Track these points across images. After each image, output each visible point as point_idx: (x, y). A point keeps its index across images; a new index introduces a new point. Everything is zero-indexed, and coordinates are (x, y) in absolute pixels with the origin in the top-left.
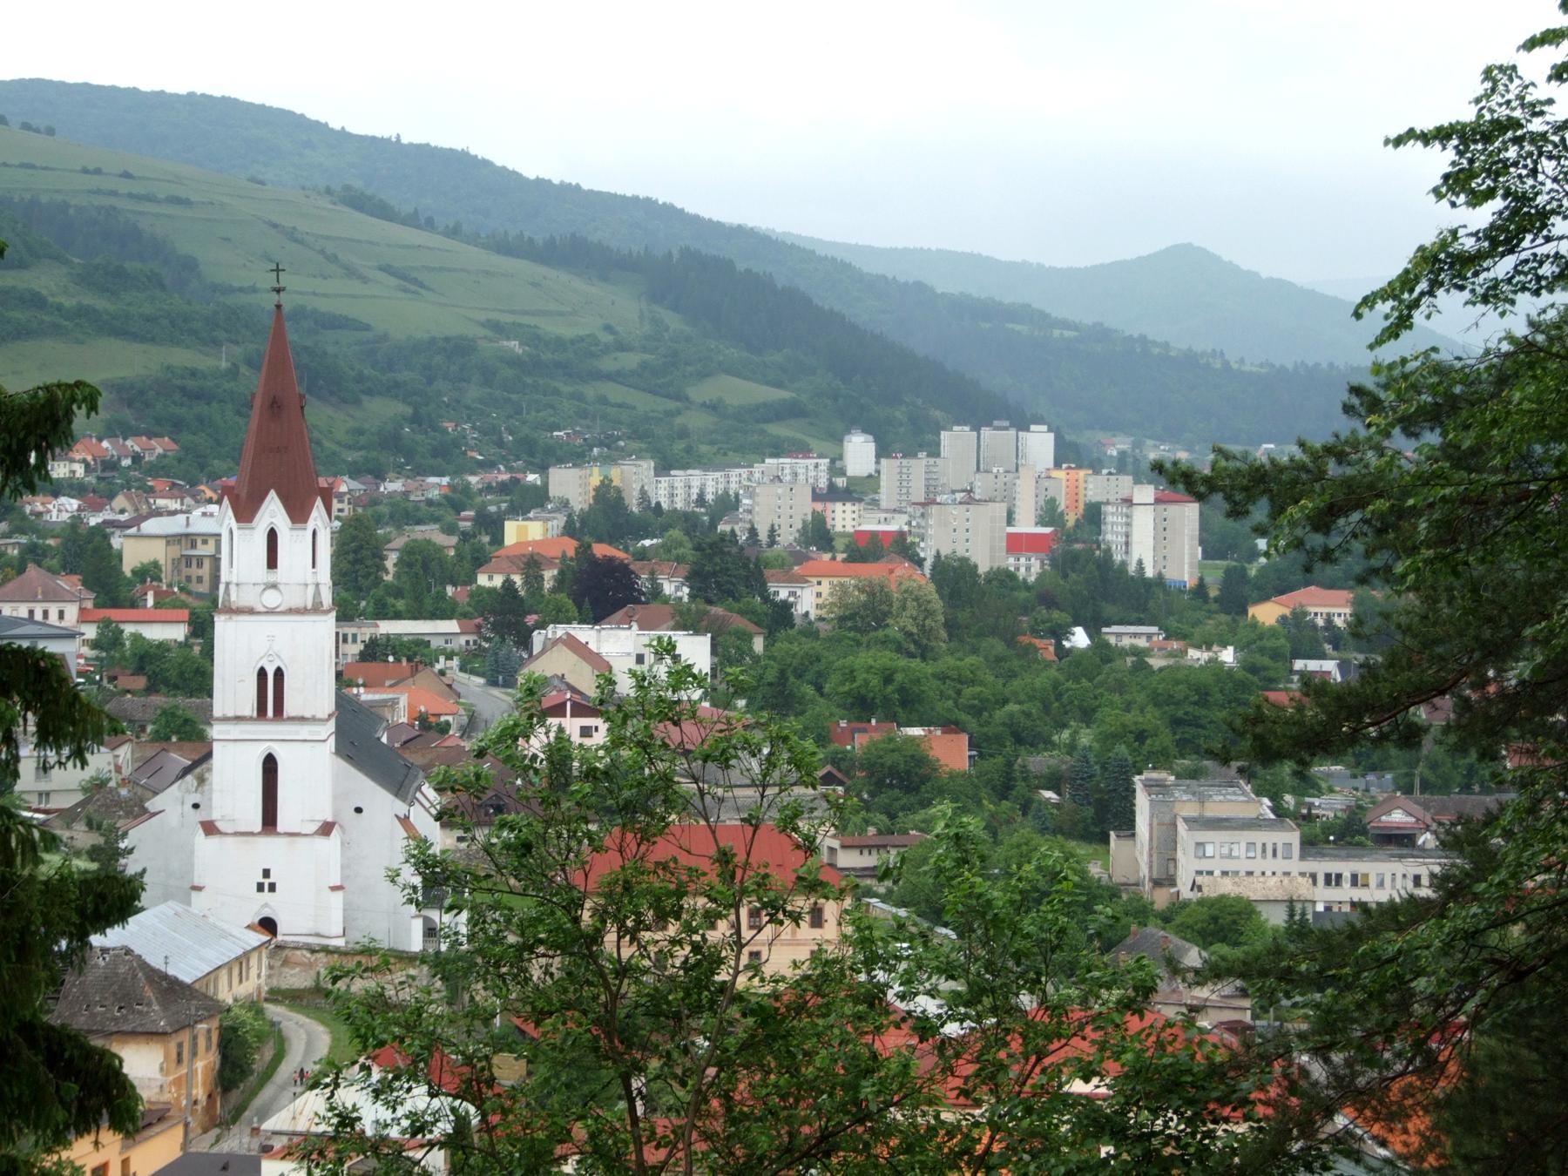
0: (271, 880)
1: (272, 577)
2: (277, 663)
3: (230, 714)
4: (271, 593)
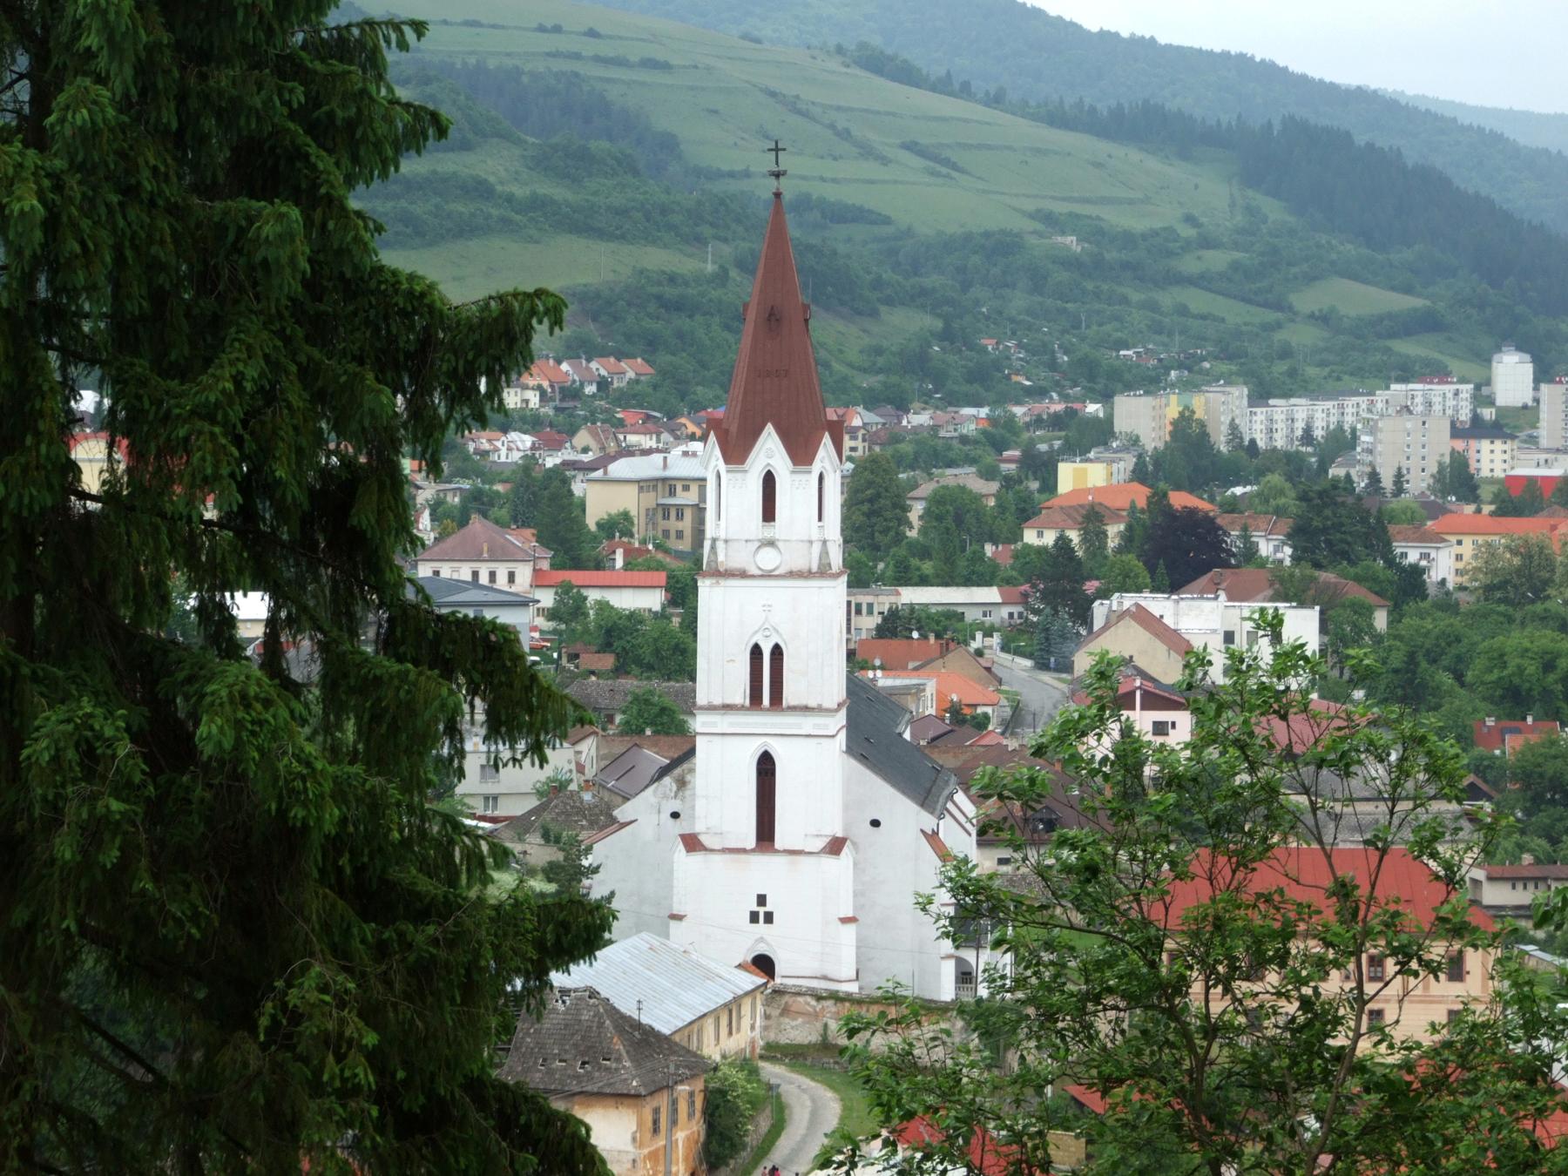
0: (768, 909)
1: (769, 532)
3: (717, 701)
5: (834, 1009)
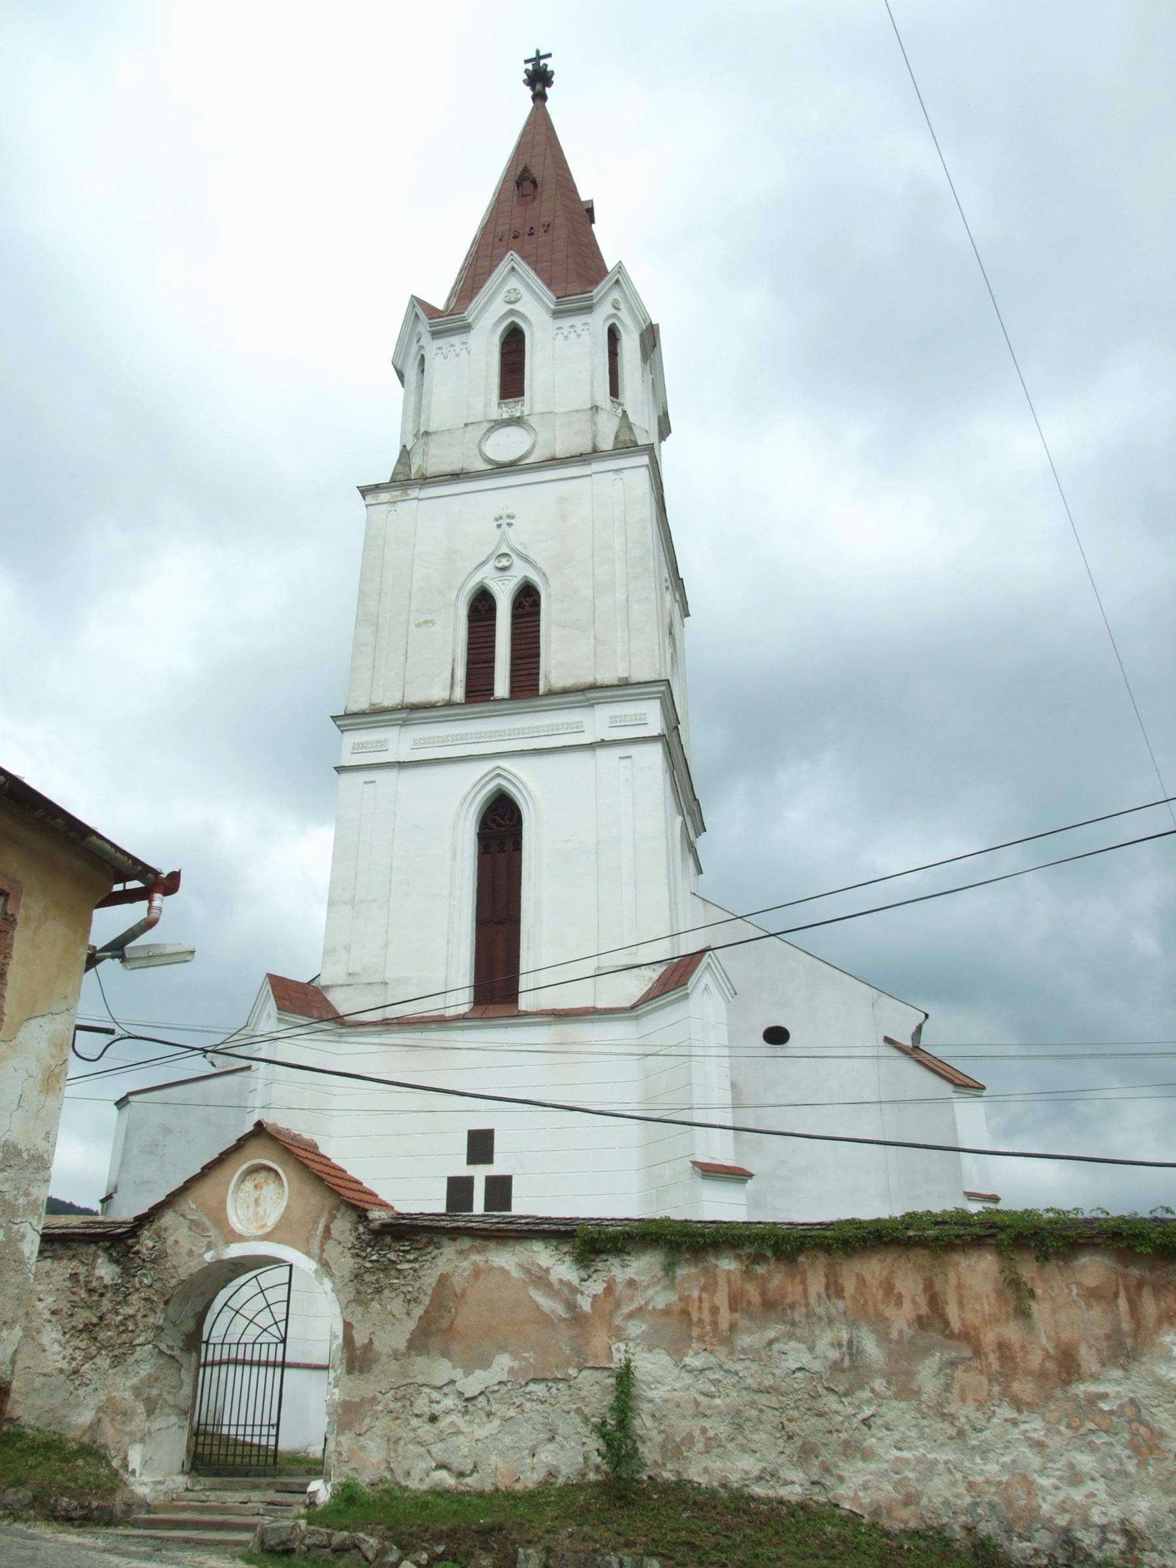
0: (497, 1168)
2: (520, 572)
4: (513, 432)
5: (662, 1299)
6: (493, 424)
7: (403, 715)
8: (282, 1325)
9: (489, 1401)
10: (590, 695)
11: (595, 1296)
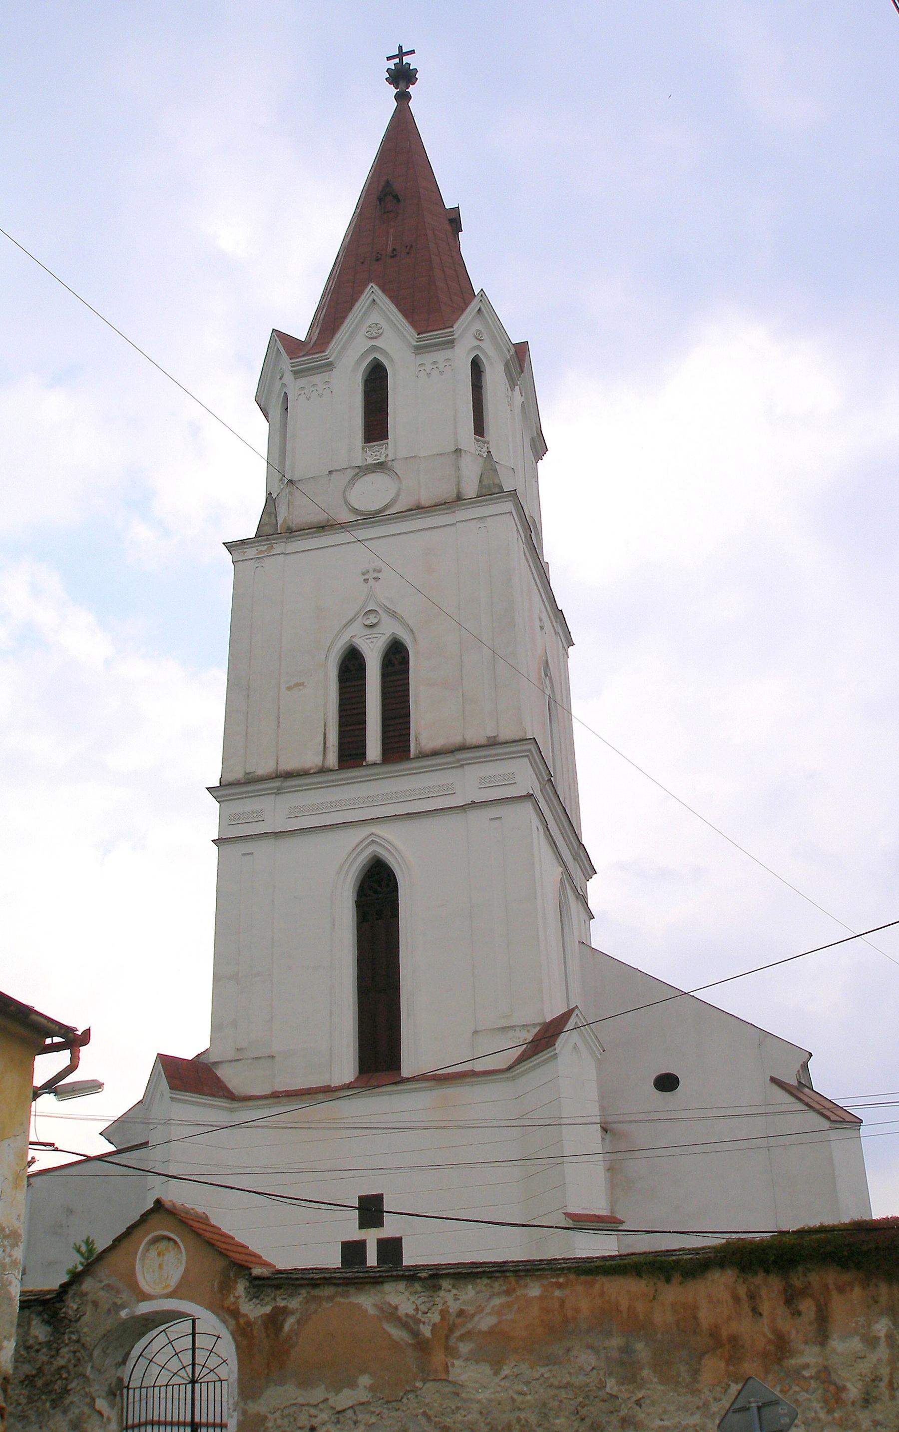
2: (388, 629)
4: (378, 480)
6: (357, 470)
7: (277, 783)
8: (189, 1369)
9: (355, 1412)
10: (460, 756)
11: (434, 1325)
